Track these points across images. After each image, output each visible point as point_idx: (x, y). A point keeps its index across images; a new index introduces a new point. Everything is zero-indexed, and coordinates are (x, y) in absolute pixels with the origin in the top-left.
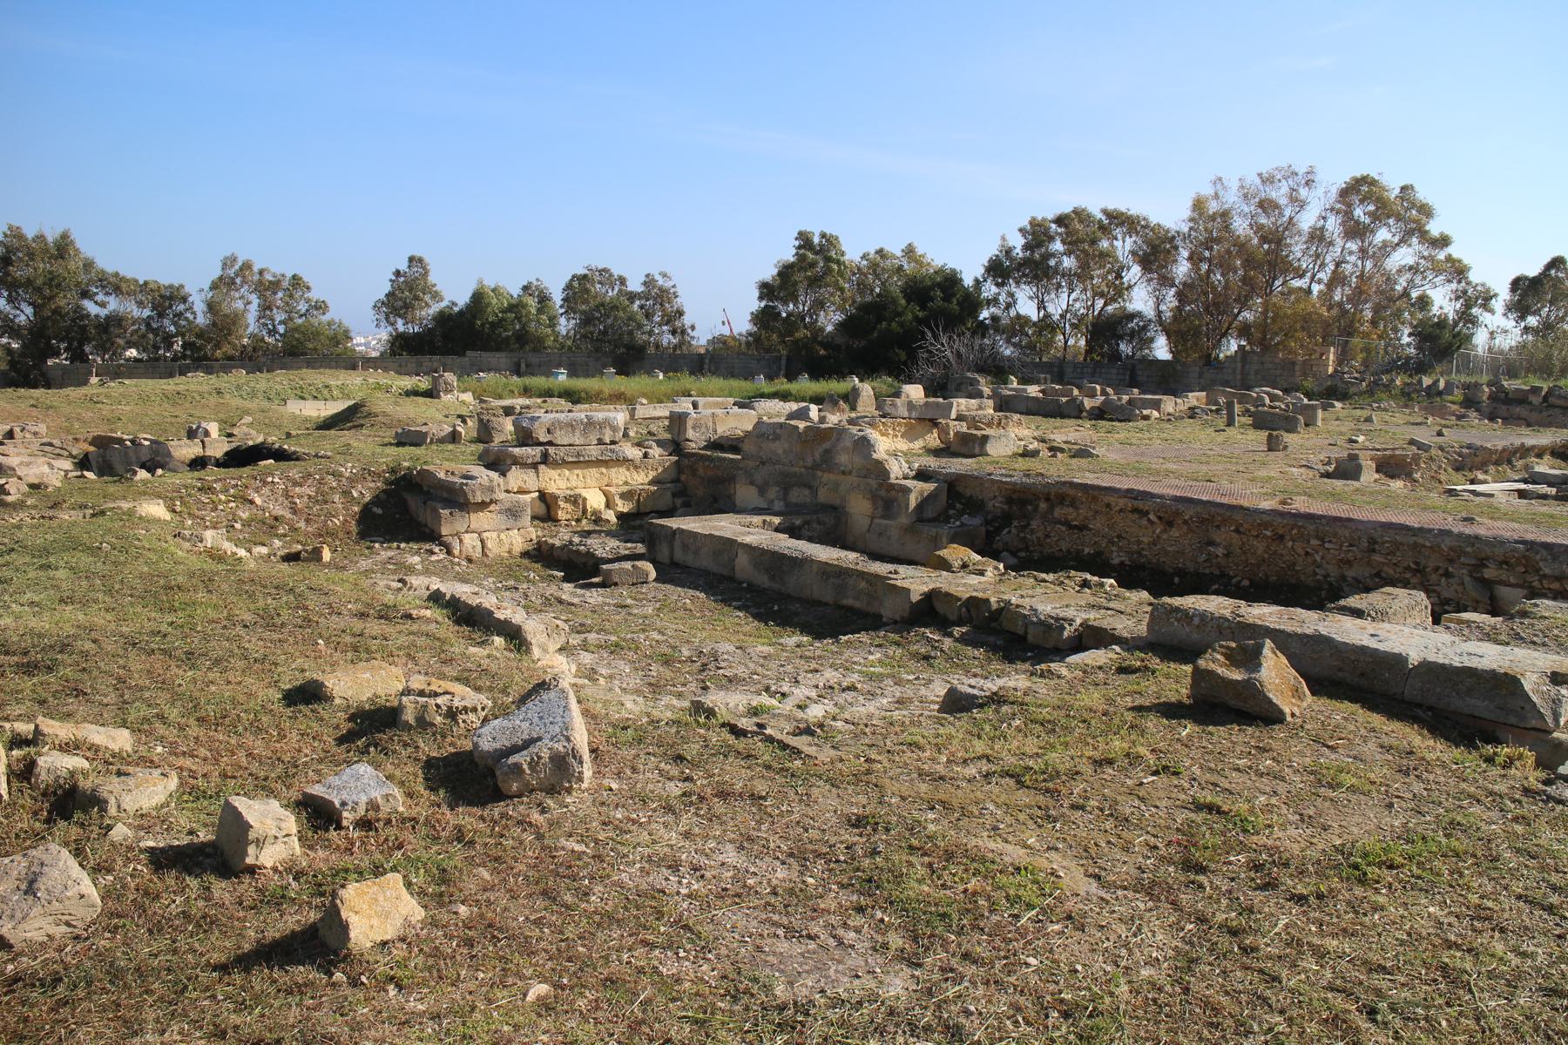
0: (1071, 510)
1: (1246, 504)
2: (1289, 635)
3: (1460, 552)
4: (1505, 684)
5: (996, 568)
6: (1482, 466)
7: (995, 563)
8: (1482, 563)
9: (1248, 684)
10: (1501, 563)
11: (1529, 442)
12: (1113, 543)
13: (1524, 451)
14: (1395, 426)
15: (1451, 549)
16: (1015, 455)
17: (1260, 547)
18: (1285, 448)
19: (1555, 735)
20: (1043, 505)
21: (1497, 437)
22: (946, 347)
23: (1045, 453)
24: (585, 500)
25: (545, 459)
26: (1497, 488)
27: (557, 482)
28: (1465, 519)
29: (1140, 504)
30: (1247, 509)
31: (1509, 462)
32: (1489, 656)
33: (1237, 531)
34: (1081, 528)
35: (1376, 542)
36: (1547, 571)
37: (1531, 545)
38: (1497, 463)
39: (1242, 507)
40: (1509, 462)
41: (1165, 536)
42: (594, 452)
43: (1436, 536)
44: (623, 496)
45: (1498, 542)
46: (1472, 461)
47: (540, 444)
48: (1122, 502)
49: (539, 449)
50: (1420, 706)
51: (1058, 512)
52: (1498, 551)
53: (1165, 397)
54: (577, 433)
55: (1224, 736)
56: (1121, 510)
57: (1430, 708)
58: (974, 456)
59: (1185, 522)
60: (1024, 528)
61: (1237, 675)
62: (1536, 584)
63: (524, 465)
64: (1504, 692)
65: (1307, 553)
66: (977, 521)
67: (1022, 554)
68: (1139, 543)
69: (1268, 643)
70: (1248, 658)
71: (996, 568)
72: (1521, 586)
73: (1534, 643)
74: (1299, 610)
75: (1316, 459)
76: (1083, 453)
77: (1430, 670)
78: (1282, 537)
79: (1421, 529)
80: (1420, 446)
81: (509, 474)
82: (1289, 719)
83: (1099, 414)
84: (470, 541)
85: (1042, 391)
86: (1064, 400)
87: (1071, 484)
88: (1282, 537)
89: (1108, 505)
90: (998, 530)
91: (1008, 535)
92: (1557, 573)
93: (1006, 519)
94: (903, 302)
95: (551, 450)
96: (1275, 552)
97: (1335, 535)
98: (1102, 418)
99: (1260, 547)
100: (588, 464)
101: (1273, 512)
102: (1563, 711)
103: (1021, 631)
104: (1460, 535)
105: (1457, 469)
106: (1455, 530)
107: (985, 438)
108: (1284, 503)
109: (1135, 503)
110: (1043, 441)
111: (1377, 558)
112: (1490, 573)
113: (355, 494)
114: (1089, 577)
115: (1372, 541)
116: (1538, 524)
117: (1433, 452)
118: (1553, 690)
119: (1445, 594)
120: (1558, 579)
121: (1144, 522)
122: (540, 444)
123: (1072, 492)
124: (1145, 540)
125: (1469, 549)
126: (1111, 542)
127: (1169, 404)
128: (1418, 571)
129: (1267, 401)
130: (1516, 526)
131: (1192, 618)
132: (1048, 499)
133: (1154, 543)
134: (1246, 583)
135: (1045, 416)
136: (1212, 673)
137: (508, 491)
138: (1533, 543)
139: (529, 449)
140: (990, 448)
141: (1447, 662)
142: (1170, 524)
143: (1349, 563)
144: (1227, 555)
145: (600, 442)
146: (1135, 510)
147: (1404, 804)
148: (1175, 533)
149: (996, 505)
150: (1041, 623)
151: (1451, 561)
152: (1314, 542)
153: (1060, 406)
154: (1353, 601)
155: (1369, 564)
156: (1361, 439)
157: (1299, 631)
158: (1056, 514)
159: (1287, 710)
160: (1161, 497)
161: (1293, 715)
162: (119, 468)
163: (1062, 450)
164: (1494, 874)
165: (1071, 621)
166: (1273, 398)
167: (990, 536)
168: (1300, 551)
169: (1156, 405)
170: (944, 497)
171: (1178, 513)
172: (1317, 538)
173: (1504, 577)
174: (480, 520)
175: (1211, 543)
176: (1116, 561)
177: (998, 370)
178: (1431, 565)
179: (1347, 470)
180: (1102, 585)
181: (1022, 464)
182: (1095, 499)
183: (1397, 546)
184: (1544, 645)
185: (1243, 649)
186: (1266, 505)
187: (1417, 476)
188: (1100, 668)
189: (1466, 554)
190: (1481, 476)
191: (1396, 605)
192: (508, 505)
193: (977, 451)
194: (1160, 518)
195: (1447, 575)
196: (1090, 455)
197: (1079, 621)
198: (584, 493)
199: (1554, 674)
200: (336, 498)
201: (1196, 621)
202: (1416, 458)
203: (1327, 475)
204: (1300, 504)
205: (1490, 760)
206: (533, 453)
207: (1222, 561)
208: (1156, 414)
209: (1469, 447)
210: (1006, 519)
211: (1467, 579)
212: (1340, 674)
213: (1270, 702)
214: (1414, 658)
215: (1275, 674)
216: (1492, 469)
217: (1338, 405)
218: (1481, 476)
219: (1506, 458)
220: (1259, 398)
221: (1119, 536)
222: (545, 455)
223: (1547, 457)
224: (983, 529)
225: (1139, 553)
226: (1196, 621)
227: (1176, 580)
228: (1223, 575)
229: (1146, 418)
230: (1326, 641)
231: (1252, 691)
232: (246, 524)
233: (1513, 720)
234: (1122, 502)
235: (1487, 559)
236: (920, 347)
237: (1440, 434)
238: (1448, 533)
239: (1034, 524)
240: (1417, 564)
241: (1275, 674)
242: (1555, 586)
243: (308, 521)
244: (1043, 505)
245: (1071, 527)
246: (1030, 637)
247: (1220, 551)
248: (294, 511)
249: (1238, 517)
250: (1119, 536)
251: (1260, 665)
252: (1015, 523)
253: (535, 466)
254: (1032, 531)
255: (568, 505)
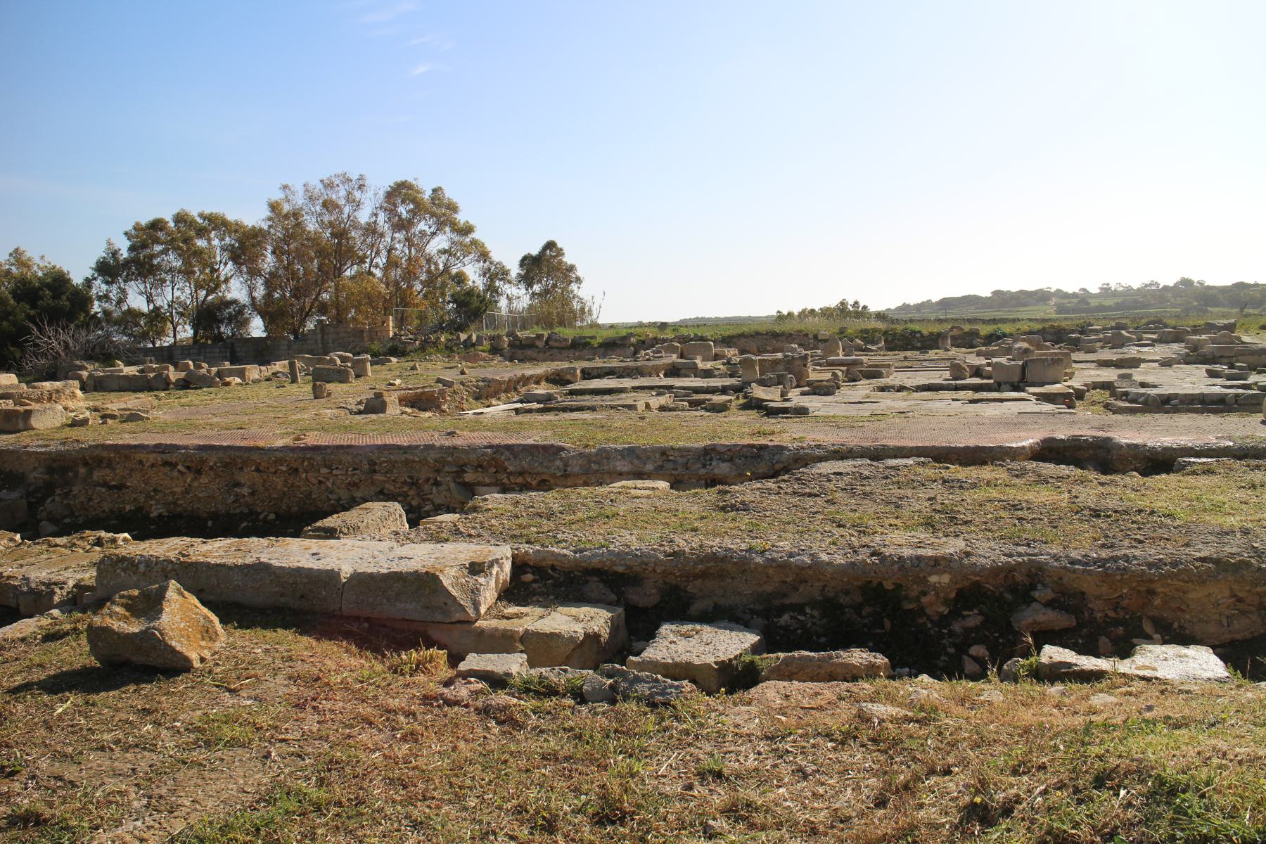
0: (108, 471)
1: (261, 444)
2: (230, 568)
3: (444, 463)
4: (424, 584)
5: (12, 540)
6: (495, 395)
7: (11, 535)
8: (461, 470)
9: (146, 635)
10: (476, 467)
11: (528, 372)
12: (151, 498)
13: (525, 380)
14: (433, 371)
15: (436, 460)
16: (64, 426)
17: (279, 482)
18: (329, 395)
19: (477, 624)
20: (82, 470)
21: (503, 371)
22: (54, 340)
23: (94, 419)
26: (499, 409)
28: (449, 434)
29: (167, 457)
30: (263, 449)
31: (516, 389)
32: (418, 555)
33: (258, 470)
34: (120, 487)
35: (375, 464)
36: (511, 468)
37: (497, 449)
38: (506, 391)
39: (258, 448)
40: (516, 389)
41: (196, 484)
43: (422, 451)
45: (472, 449)
46: (486, 392)
48: (152, 457)
50: (358, 618)
51: (97, 475)
52: (473, 457)
53: (248, 367)
55: (128, 699)
56: (153, 465)
57: (368, 619)
58: (19, 431)
59: (211, 468)
60: (66, 495)
61: (134, 628)
62: (505, 481)
64: (427, 591)
65: (320, 482)
66: (15, 495)
67: (67, 520)
68: (173, 493)
69: (173, 584)
70: (150, 605)
71: (12, 540)
72: (496, 485)
73: (470, 536)
74: (255, 539)
75: (352, 403)
76: (133, 417)
77: (362, 581)
78: (296, 470)
79: (410, 447)
80: (445, 383)
82: (197, 664)
83: (185, 385)
85: (141, 371)
86: (152, 375)
87: (104, 447)
88: (296, 470)
89: (141, 462)
90: (41, 501)
91: (53, 504)
92: (519, 469)
93: (49, 489)
94: (12, 302)
96: (293, 485)
97: (340, 462)
98: (188, 388)
99: (279, 482)
101: (286, 448)
102: (482, 599)
103: (13, 603)
104: (442, 447)
105: (477, 399)
106: (437, 444)
107: (28, 414)
108: (298, 439)
109: (164, 456)
110: (96, 410)
111: (378, 477)
112: (469, 477)
114: (103, 534)
115: (372, 463)
116: (506, 430)
117: (456, 387)
118: (471, 580)
119: (438, 501)
120: (521, 474)
121: (176, 474)
123: (105, 454)
124: (178, 490)
125: (450, 459)
126: (149, 497)
127: (254, 372)
128: (413, 484)
129: (339, 362)
130: (489, 434)
131: (137, 566)
132: (86, 464)
133: (187, 491)
134: (272, 516)
135: (135, 391)
136: (107, 630)
138: (498, 446)
140: (34, 422)
141: (375, 570)
142: (199, 472)
143: (355, 485)
144: (252, 494)
146: (166, 463)
147: (285, 748)
148: (204, 480)
149: (36, 476)
150: (32, 591)
151: (438, 471)
152: (324, 471)
153: (148, 381)
154: (329, 522)
155: (373, 483)
156: (398, 382)
157: (240, 561)
158: (95, 477)
159: (194, 656)
160: (186, 447)
161: (202, 660)
163: (113, 417)
164: (352, 824)
165: (61, 585)
166: (343, 359)
167: (32, 507)
168: (314, 481)
169: (241, 374)
171: (203, 461)
172: (325, 466)
173: (480, 479)
175: (238, 484)
176: (154, 514)
177: (105, 355)
178: (423, 476)
179: (375, 406)
180: (114, 541)
181: (68, 432)
182: (127, 457)
183: (393, 464)
184: (479, 536)
185: (145, 596)
186: (280, 443)
187: (445, 407)
188: (23, 640)
189: (448, 463)
190: (494, 402)
191: (368, 519)
193: (21, 425)
194: (188, 468)
195: (437, 483)
196: (142, 418)
197: (71, 583)
199: (472, 564)
201: (142, 568)
202: (442, 393)
203: (360, 412)
204: (312, 439)
205: (395, 670)
207: (249, 500)
208: (238, 380)
209: (483, 380)
210: (49, 489)
211: (452, 485)
212: (283, 600)
213: (173, 650)
214: (346, 570)
215: (182, 619)
216: (503, 396)
217: (394, 360)
218: (494, 402)
219: (512, 386)
220: (332, 361)
221: (155, 490)
223: (543, 383)
224: (24, 501)
225: (175, 503)
226: (142, 568)
227: (210, 523)
228: (252, 512)
229: (228, 384)
230: (261, 568)
231: (151, 642)
233: (439, 617)
234: (152, 457)
235: (465, 465)
236: (27, 341)
237: (463, 373)
238: (432, 447)
239: (76, 489)
240: (411, 477)
241: (182, 619)
242: (520, 480)
244: (82, 470)
245: (111, 488)
246: (22, 608)
247: (245, 491)
249: (255, 457)
250: (155, 490)
251: (161, 611)
252: (58, 491)
254: (75, 496)
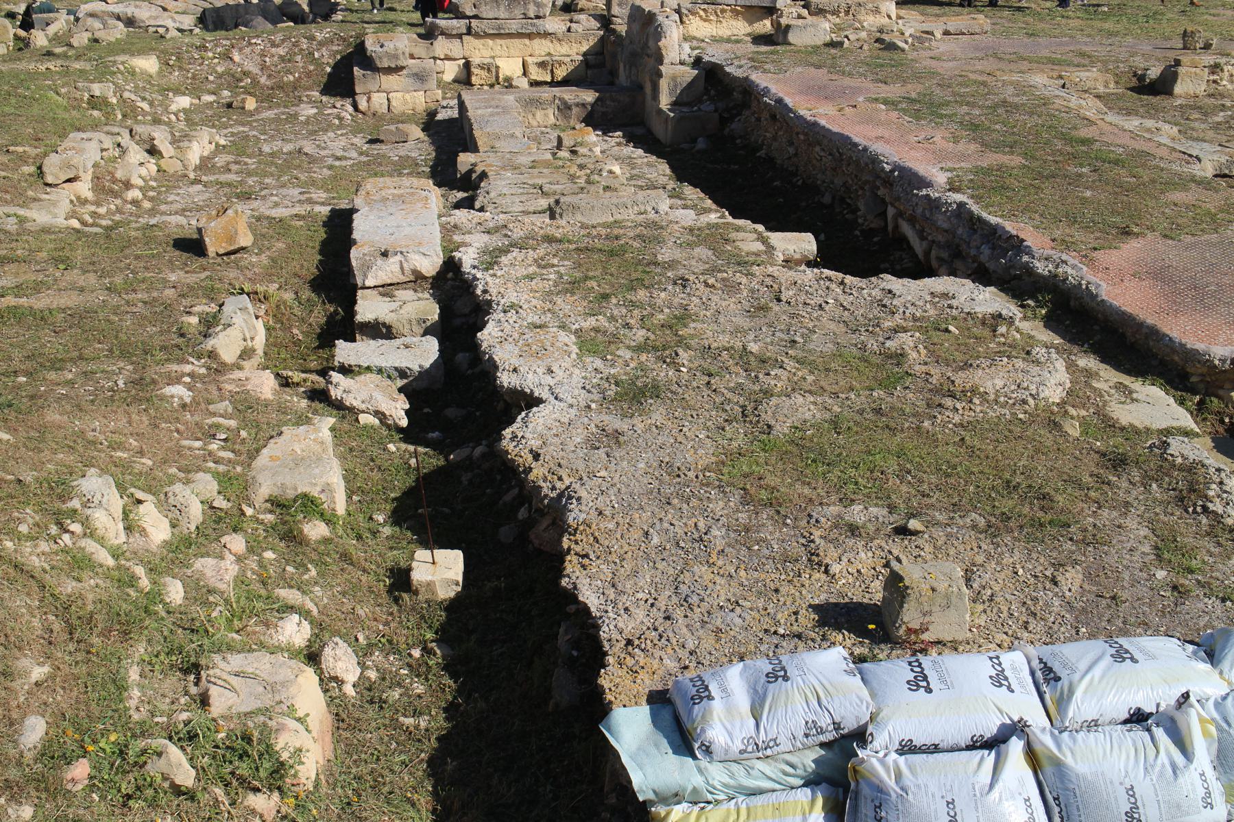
24: (497, 67)
25: (469, 31)
27: (479, 51)
42: (514, 26)
44: (542, 65)
47: (465, 17)
49: (464, 22)
54: (502, 8)
63: (449, 36)
81: (435, 43)
84: (379, 100)
95: (474, 23)
100: (510, 36)
113: (316, 55)
122: (465, 17)
137: (435, 58)
139: (455, 22)
140: (792, 37)
145: (526, 17)
162: (230, 22)
170: (702, 82)
174: (389, 81)
192: (415, 70)
198: (500, 62)
200: (298, 58)
206: (458, 25)
222: (469, 28)
224: (716, 115)
232: (220, 76)
243: (269, 76)
248: (263, 67)
253: (460, 36)
255: (484, 73)
